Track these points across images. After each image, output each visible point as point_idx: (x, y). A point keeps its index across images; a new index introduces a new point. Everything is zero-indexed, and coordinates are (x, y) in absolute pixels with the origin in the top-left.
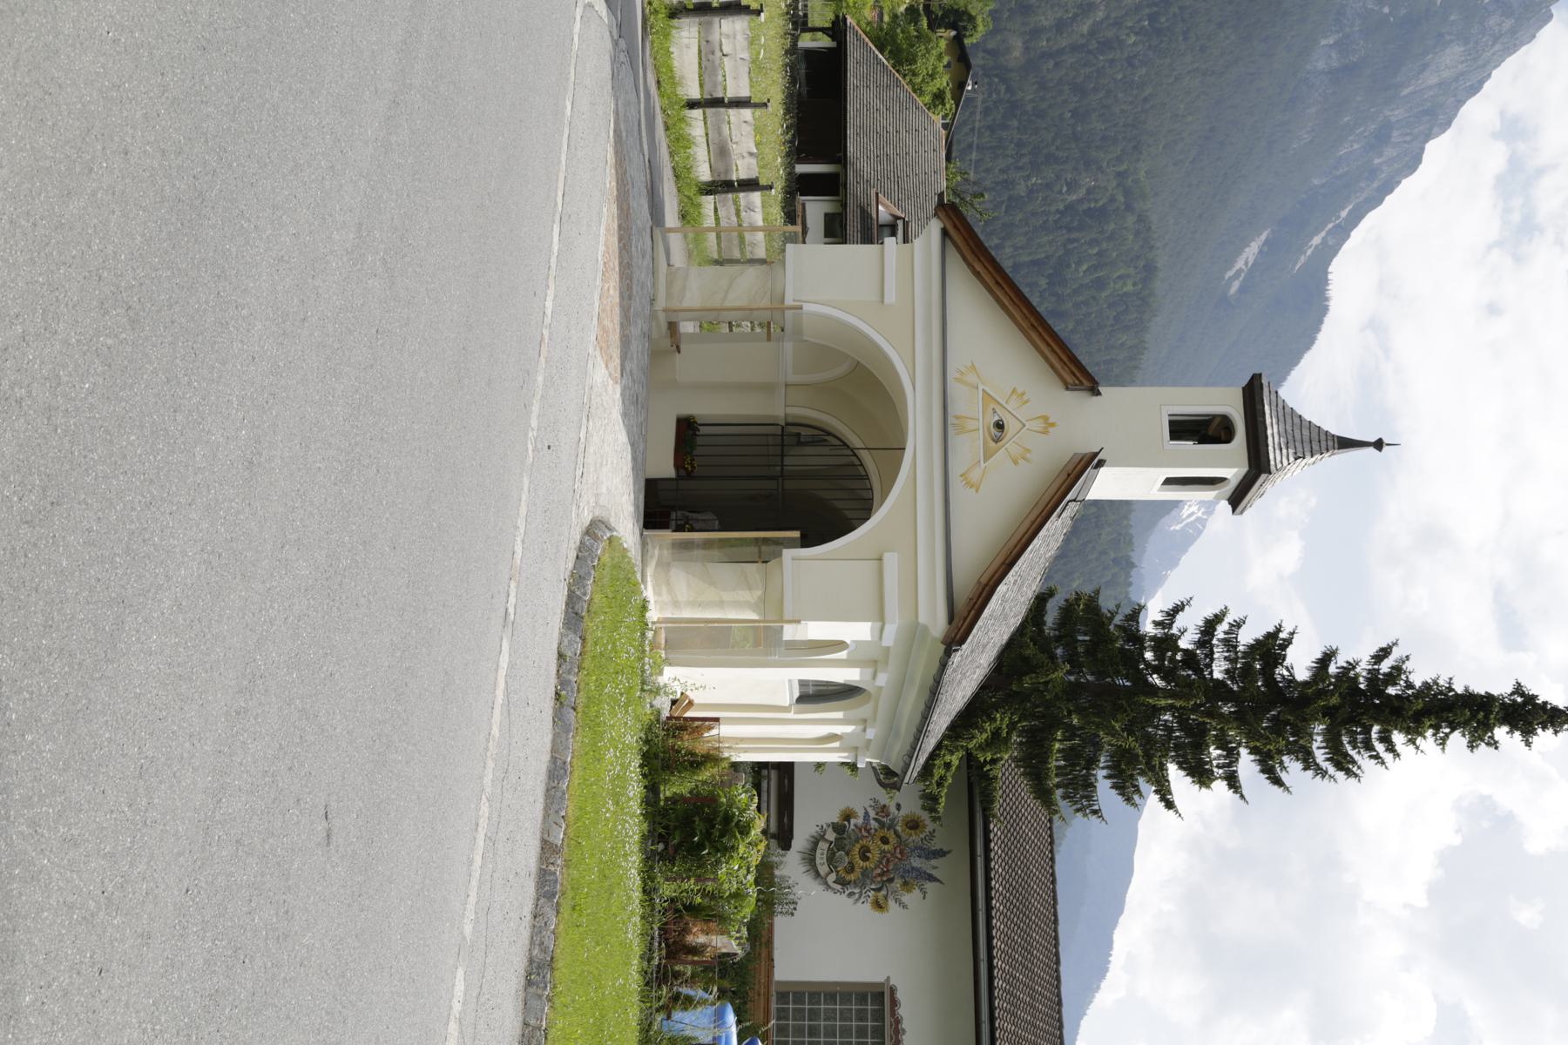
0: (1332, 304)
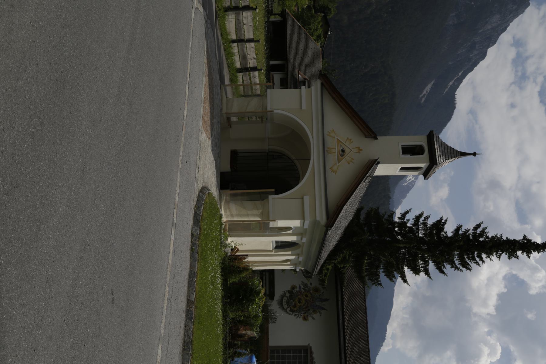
0: (457, 105)
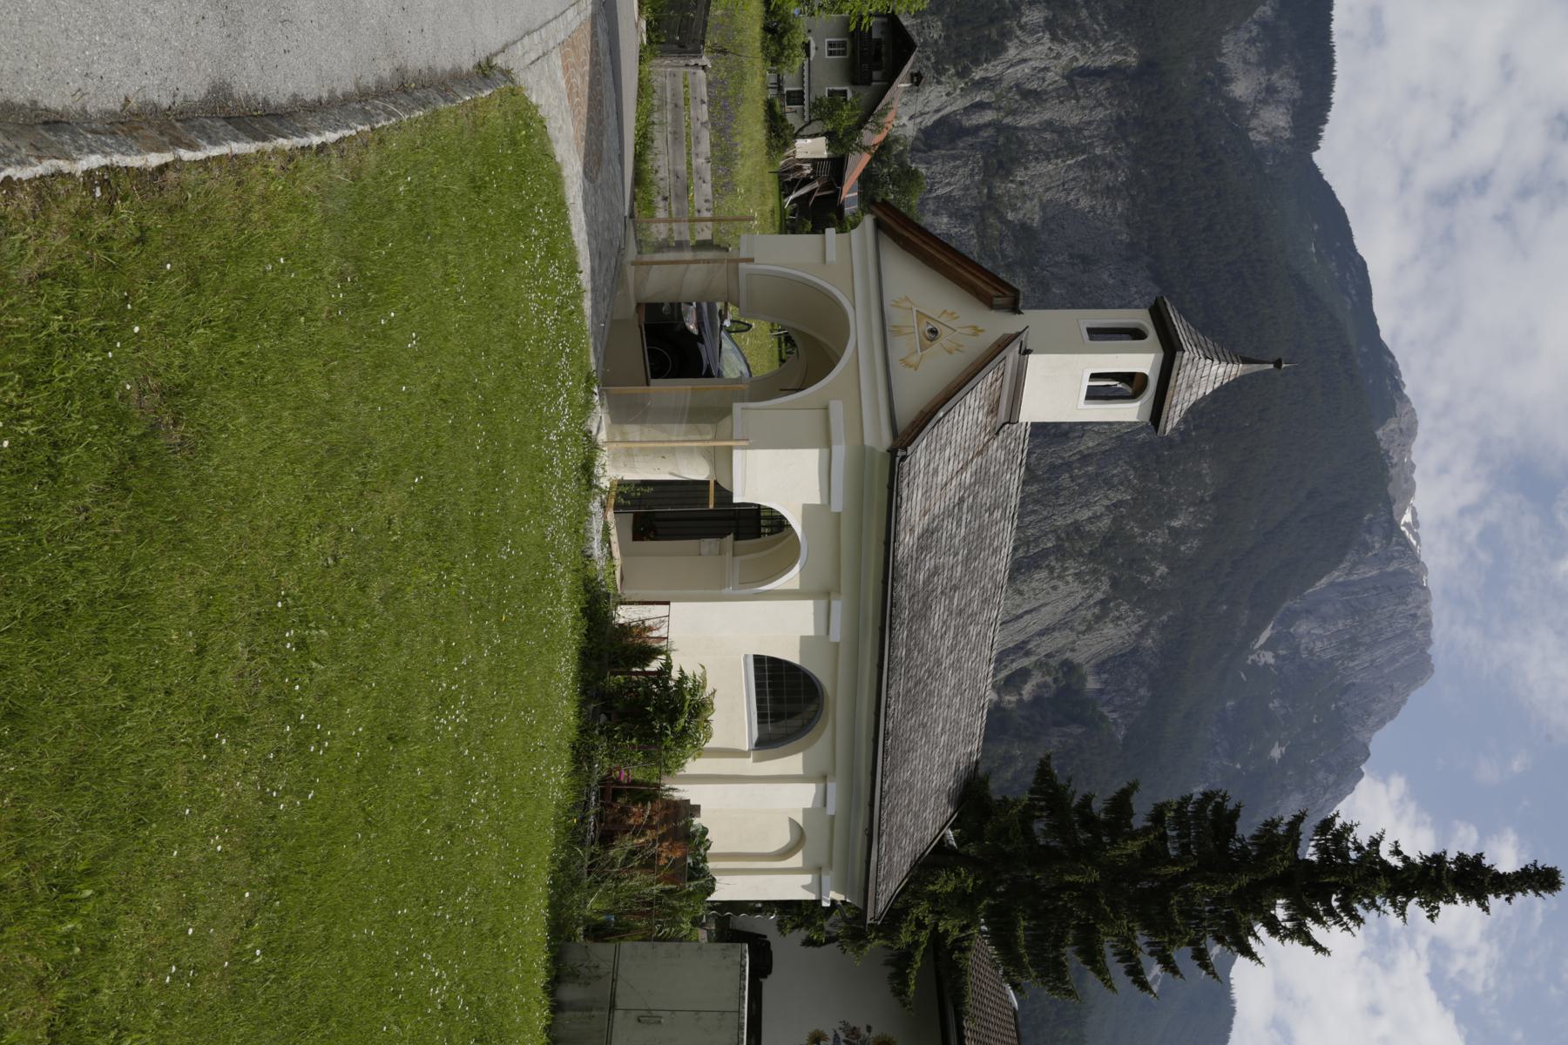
0: (1238, 1006)
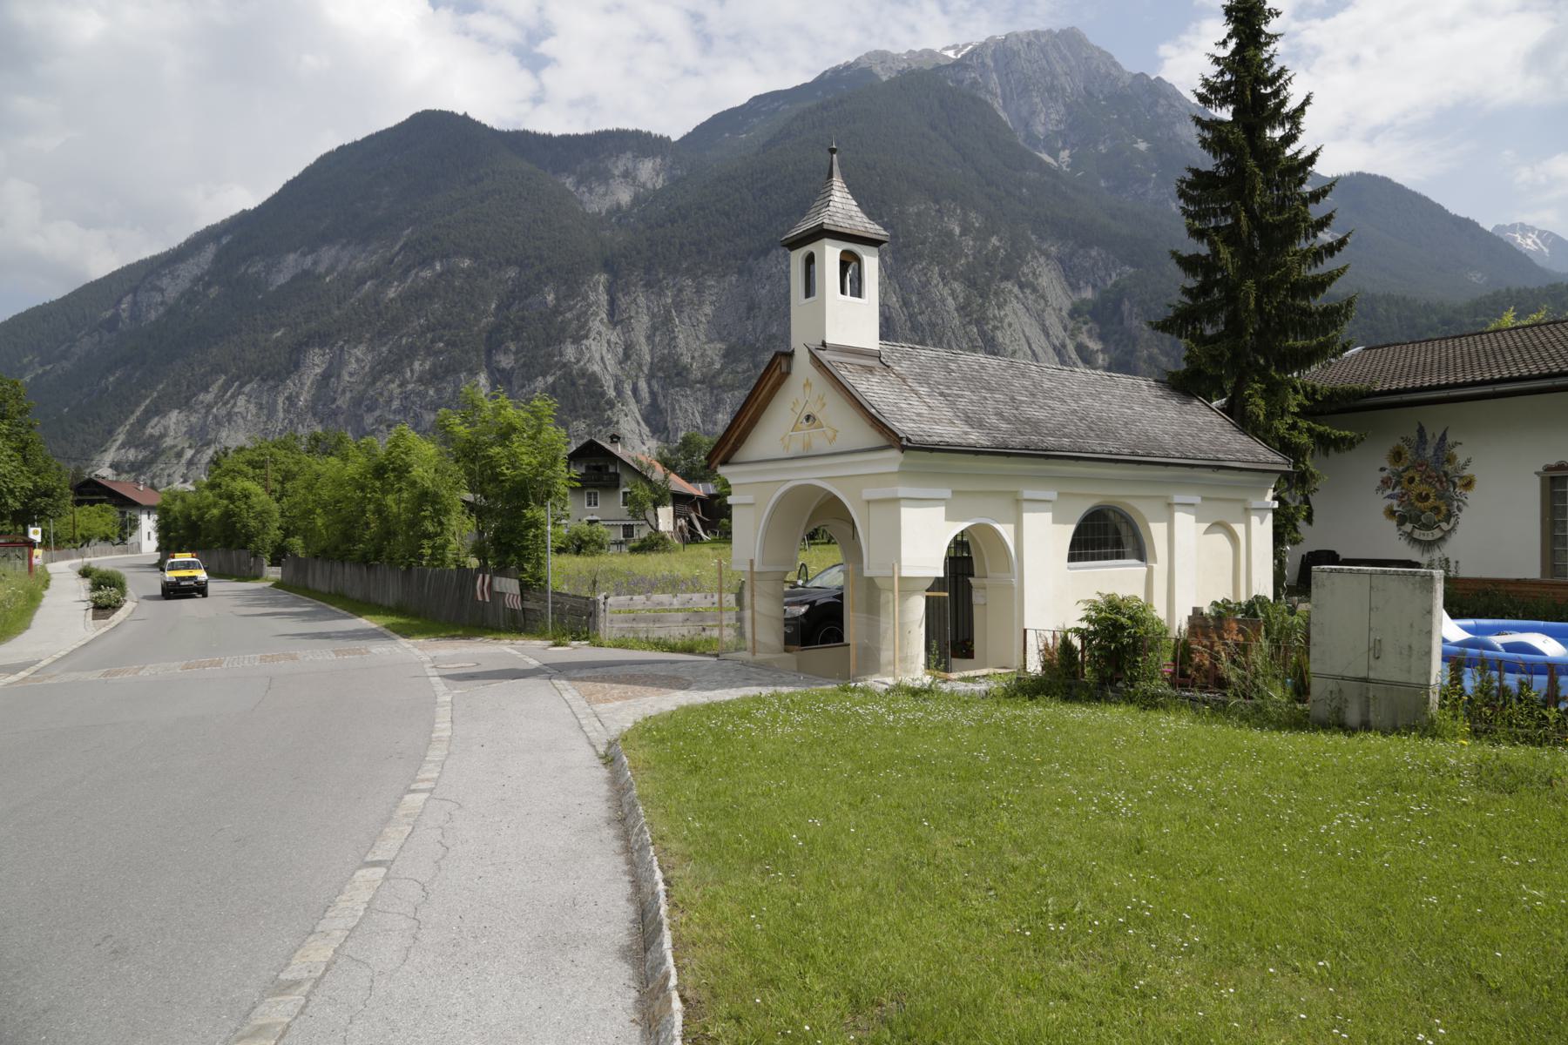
0: (1355, 170)
